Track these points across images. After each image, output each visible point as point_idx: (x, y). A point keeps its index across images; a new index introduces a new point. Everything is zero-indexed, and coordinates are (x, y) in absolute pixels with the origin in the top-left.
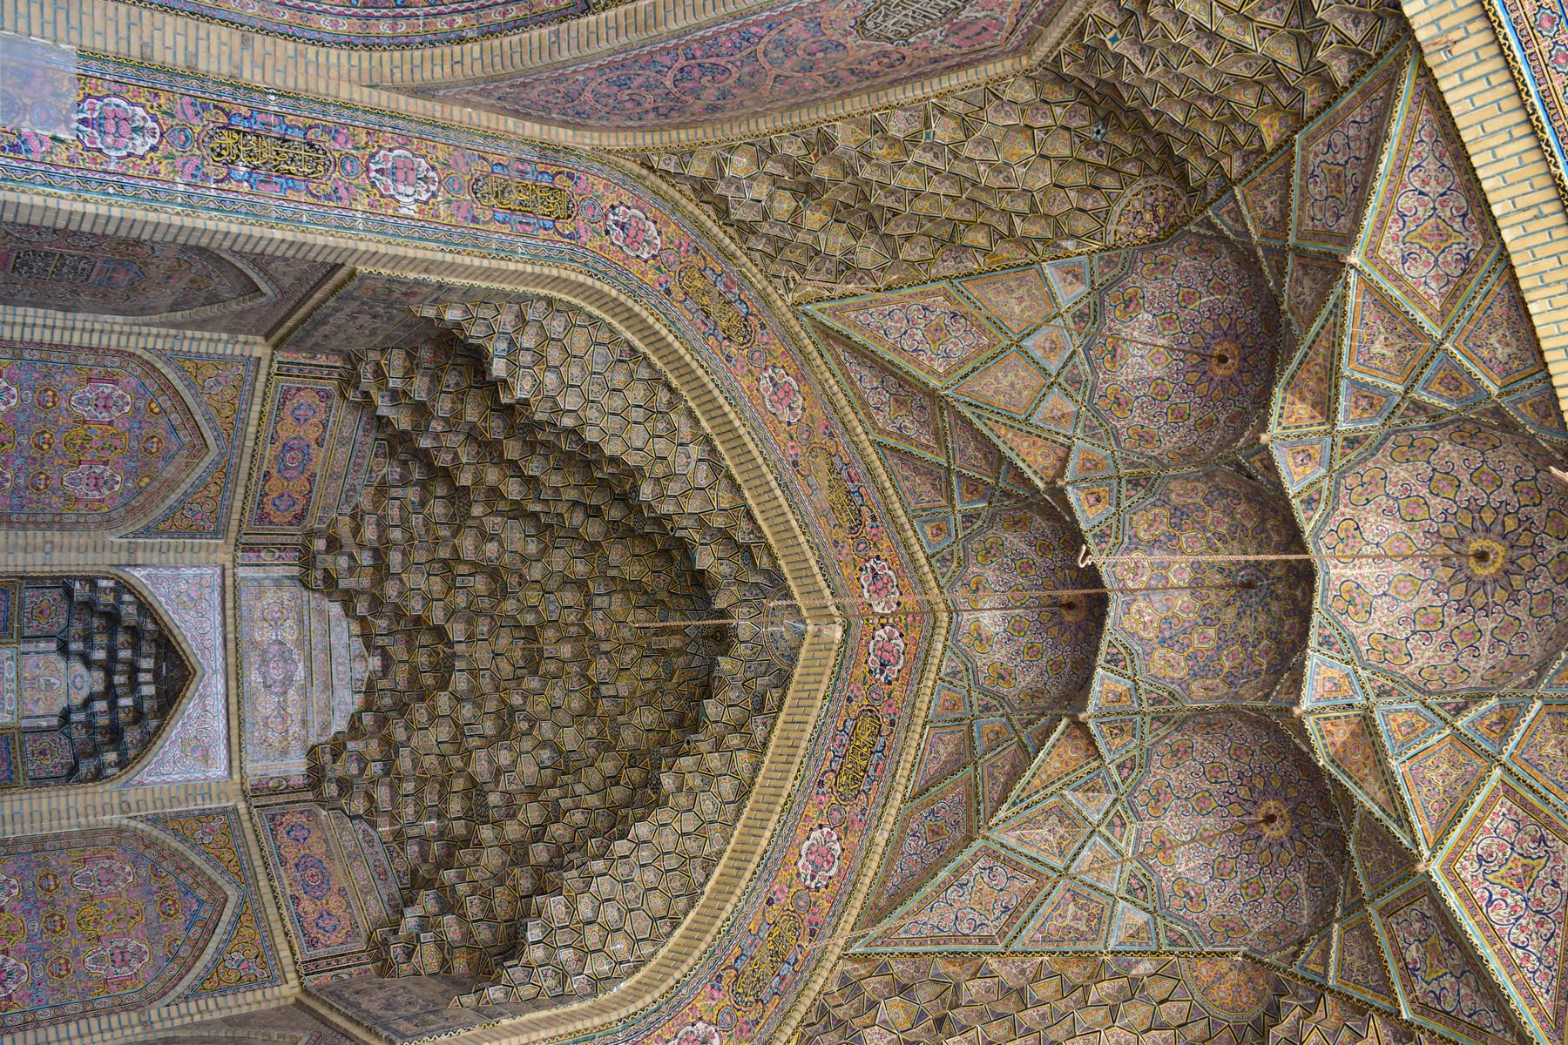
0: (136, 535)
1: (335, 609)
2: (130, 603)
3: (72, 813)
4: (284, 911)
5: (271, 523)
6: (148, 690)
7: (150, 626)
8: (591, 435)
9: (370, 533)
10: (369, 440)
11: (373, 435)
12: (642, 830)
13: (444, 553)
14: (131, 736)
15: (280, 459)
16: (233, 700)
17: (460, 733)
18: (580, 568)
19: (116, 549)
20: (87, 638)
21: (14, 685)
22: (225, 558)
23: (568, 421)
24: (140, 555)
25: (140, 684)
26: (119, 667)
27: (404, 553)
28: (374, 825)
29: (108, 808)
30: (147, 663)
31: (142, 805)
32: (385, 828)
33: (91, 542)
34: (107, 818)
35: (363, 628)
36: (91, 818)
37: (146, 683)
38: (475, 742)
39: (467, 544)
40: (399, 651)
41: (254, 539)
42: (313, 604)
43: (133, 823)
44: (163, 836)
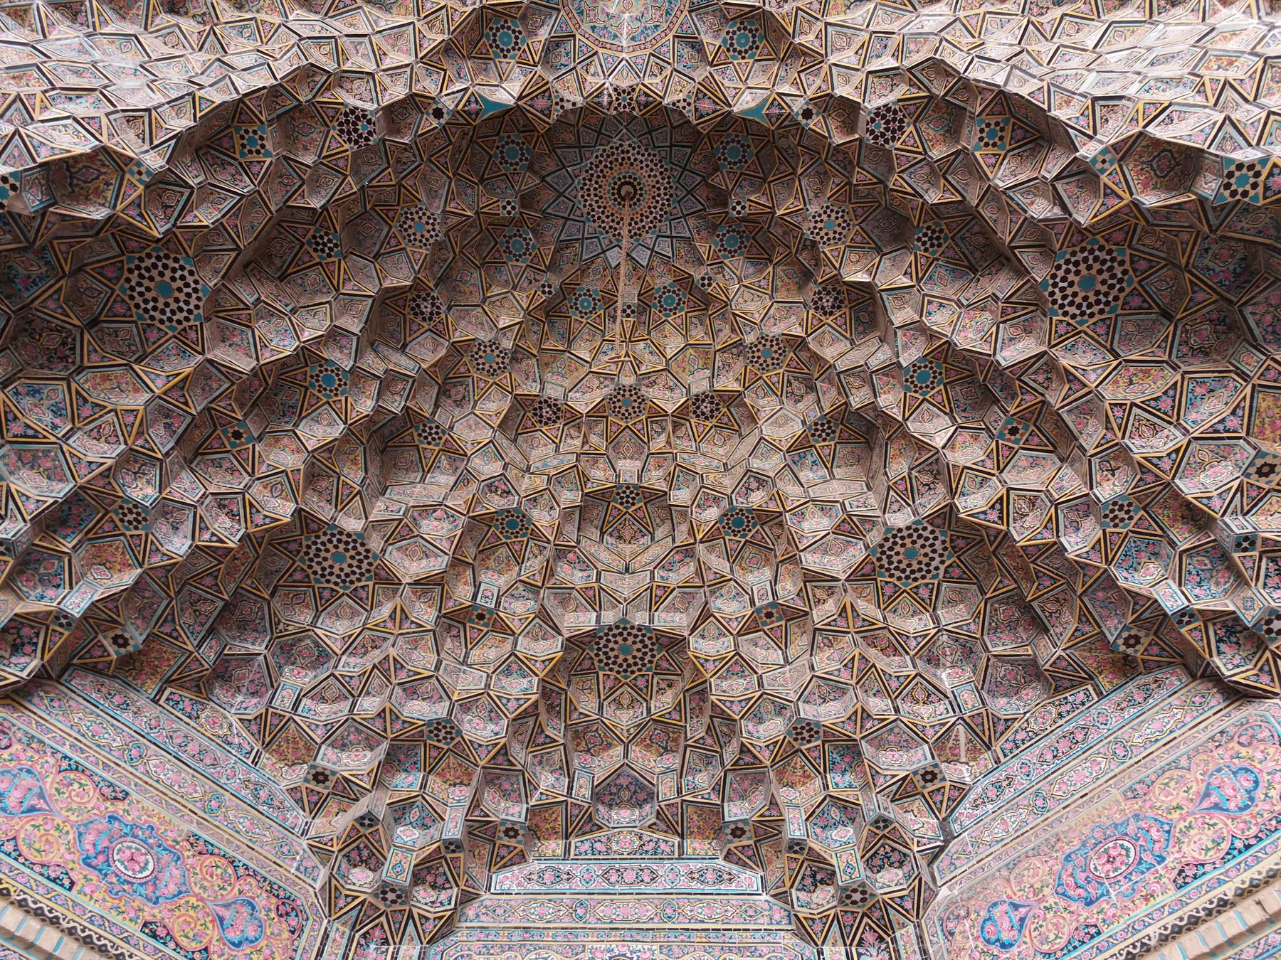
1: (507, 879)
4: (1228, 890)
8: (219, 97)
9: (357, 763)
10: (152, 711)
11: (142, 701)
12: (981, 73)
13: (426, 614)
15: (120, 888)
17: (774, 619)
18: (495, 406)
23: (181, 123)
27: (411, 689)
28: (960, 791)
32: (962, 772)
35: (553, 833)
38: (788, 589)
39: (410, 567)
40: (604, 764)
42: (486, 921)
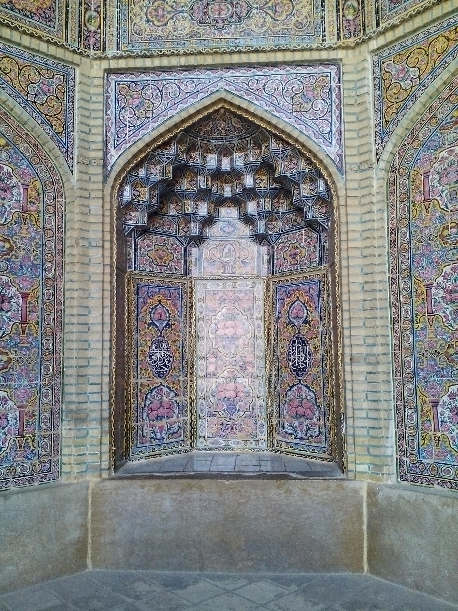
0: (69, 156)
2: (148, 170)
3: (367, 217)
5: (51, 9)
6: (239, 160)
7: (171, 151)
14: (284, 168)
16: (254, 58)
19: (86, 177)
20: (187, 219)
21: (230, 283)
22: (97, 69)
24: (92, 155)
25: (233, 168)
26: (215, 190)
29: (364, 184)
30: (212, 161)
31: (362, 150)
33: (77, 202)
34: (375, 183)
36: (374, 200)
37: (232, 161)
41: (73, 33)
43: (386, 156)
44: (405, 122)
